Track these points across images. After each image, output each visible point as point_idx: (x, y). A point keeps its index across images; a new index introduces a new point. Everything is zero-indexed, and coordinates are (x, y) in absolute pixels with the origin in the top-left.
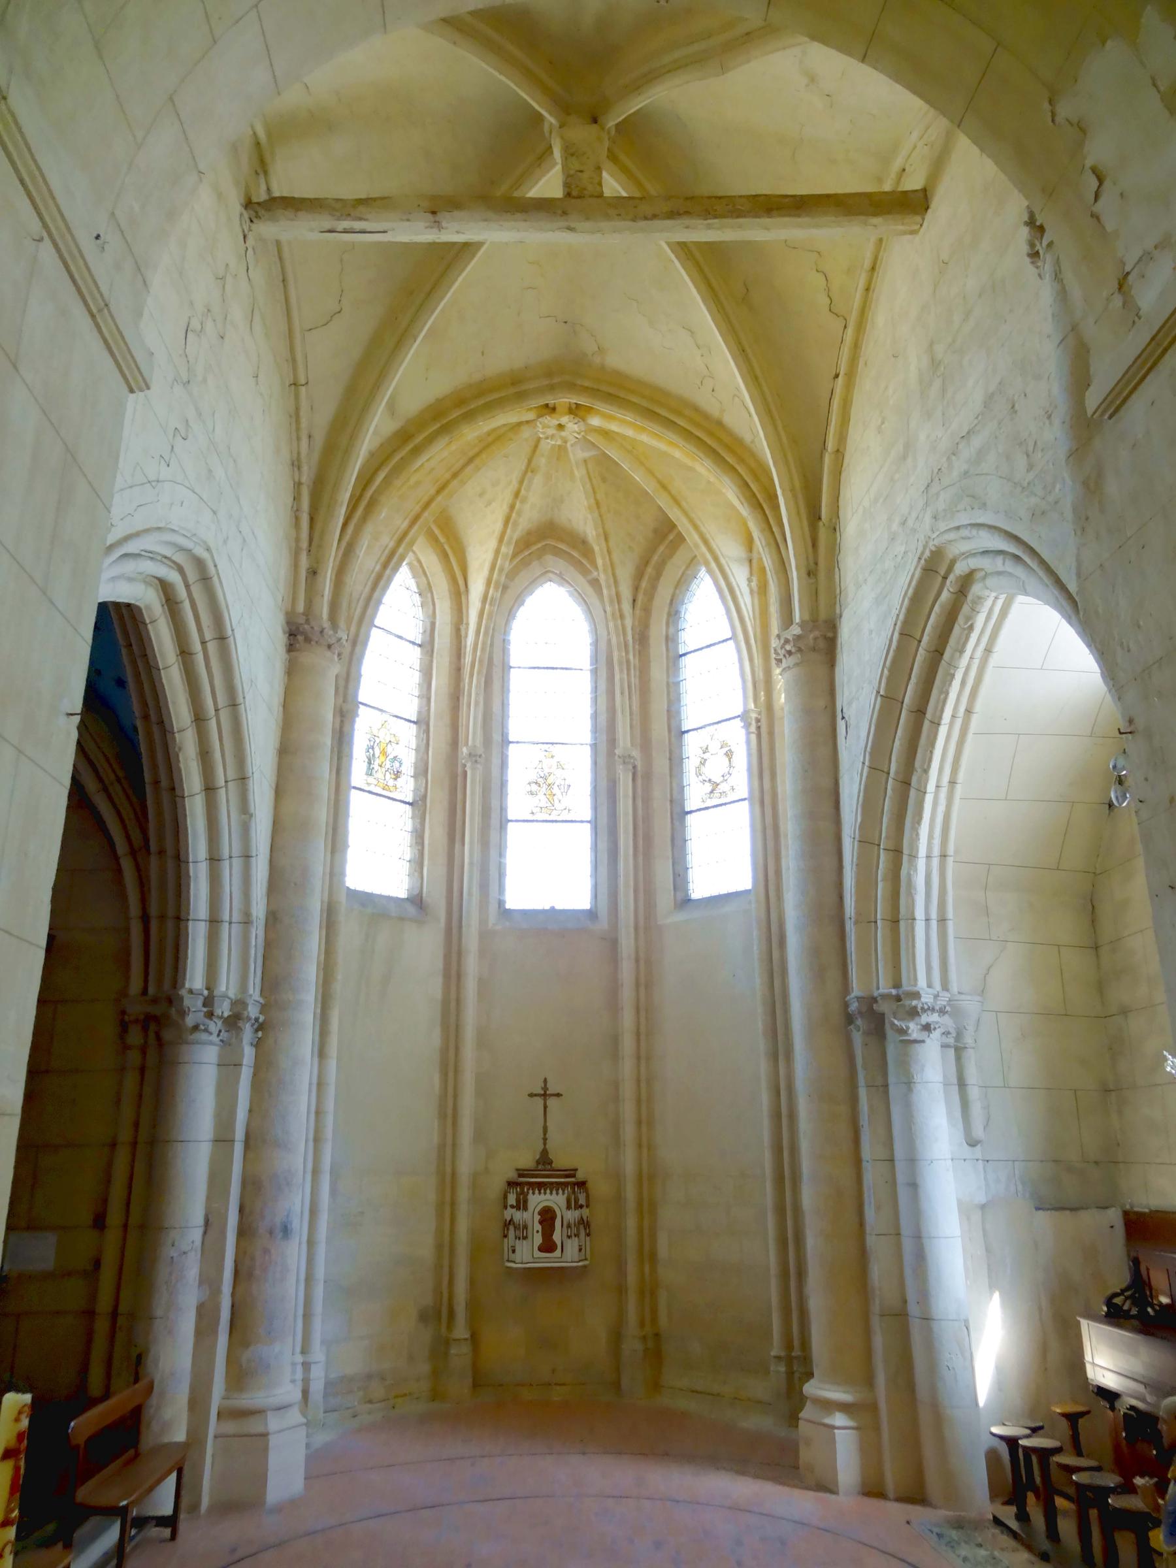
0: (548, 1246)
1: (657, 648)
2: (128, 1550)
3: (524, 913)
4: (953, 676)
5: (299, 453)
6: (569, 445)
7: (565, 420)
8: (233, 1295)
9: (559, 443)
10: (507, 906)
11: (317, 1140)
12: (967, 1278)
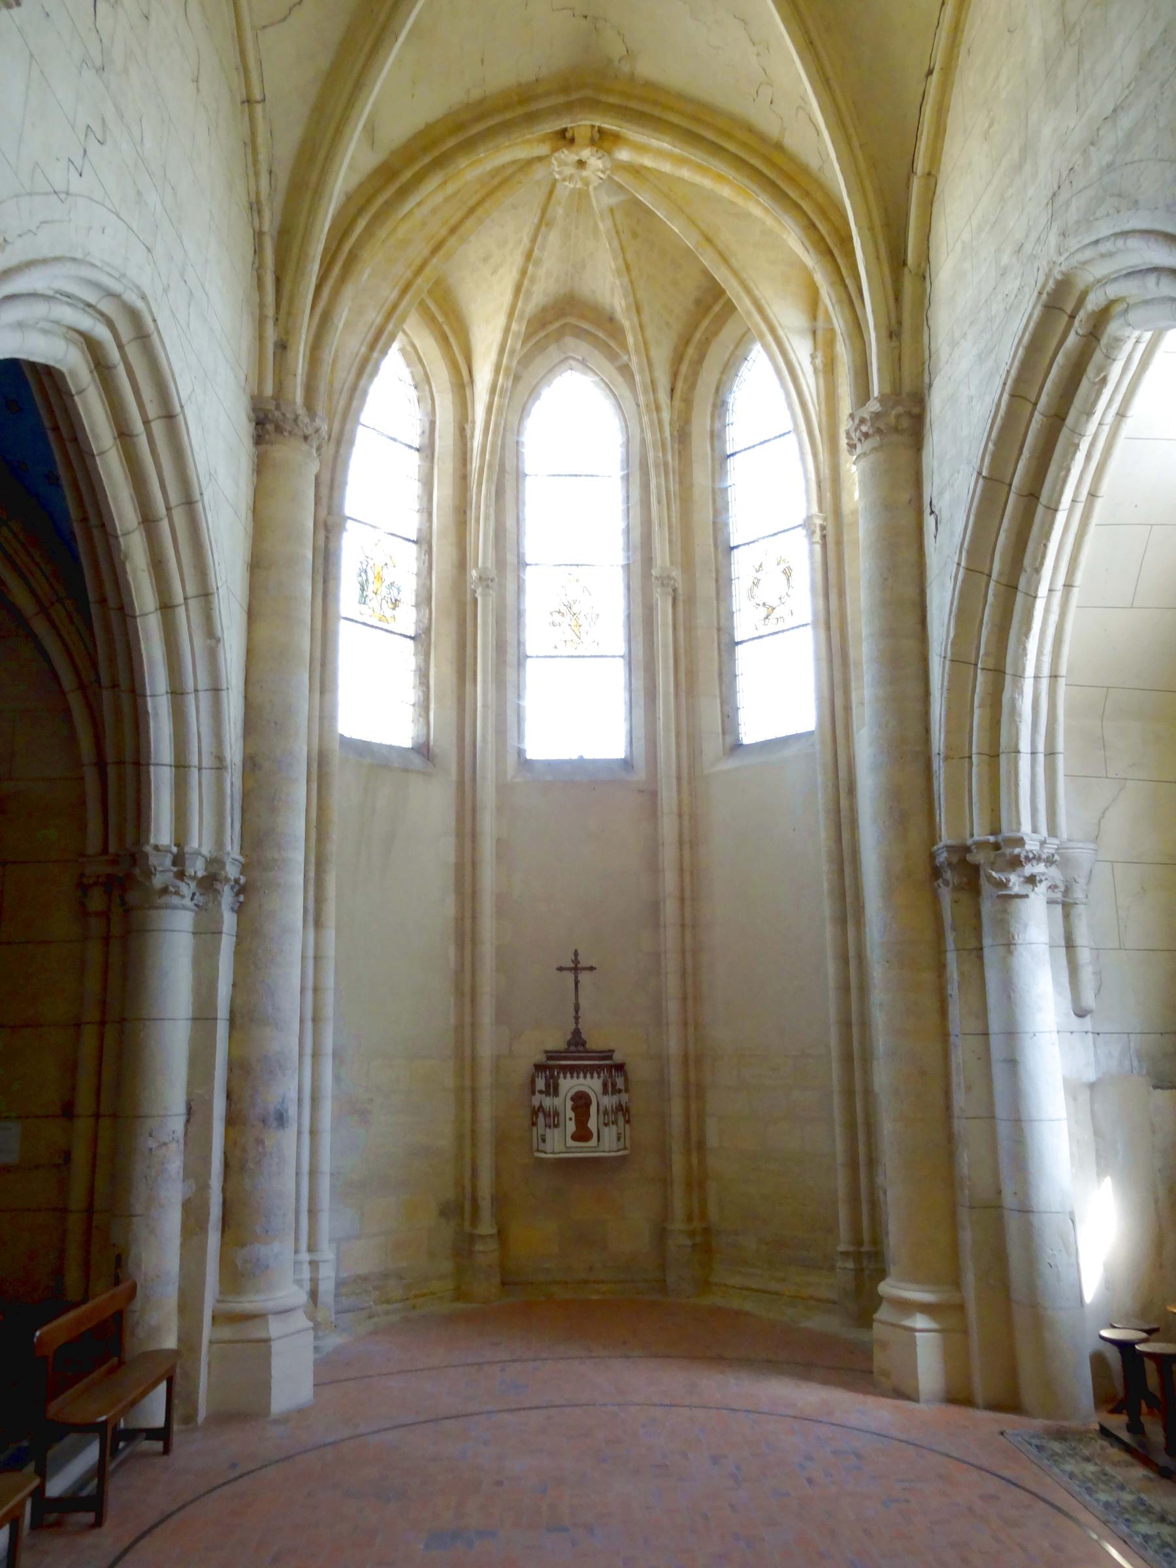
0: (582, 1134)
1: (700, 444)
2: (111, 1467)
3: (550, 765)
4: (1077, 446)
5: (258, 193)
6: (591, 188)
7: (586, 153)
8: (224, 1190)
9: (579, 185)
10: (529, 756)
12: (1072, 1165)
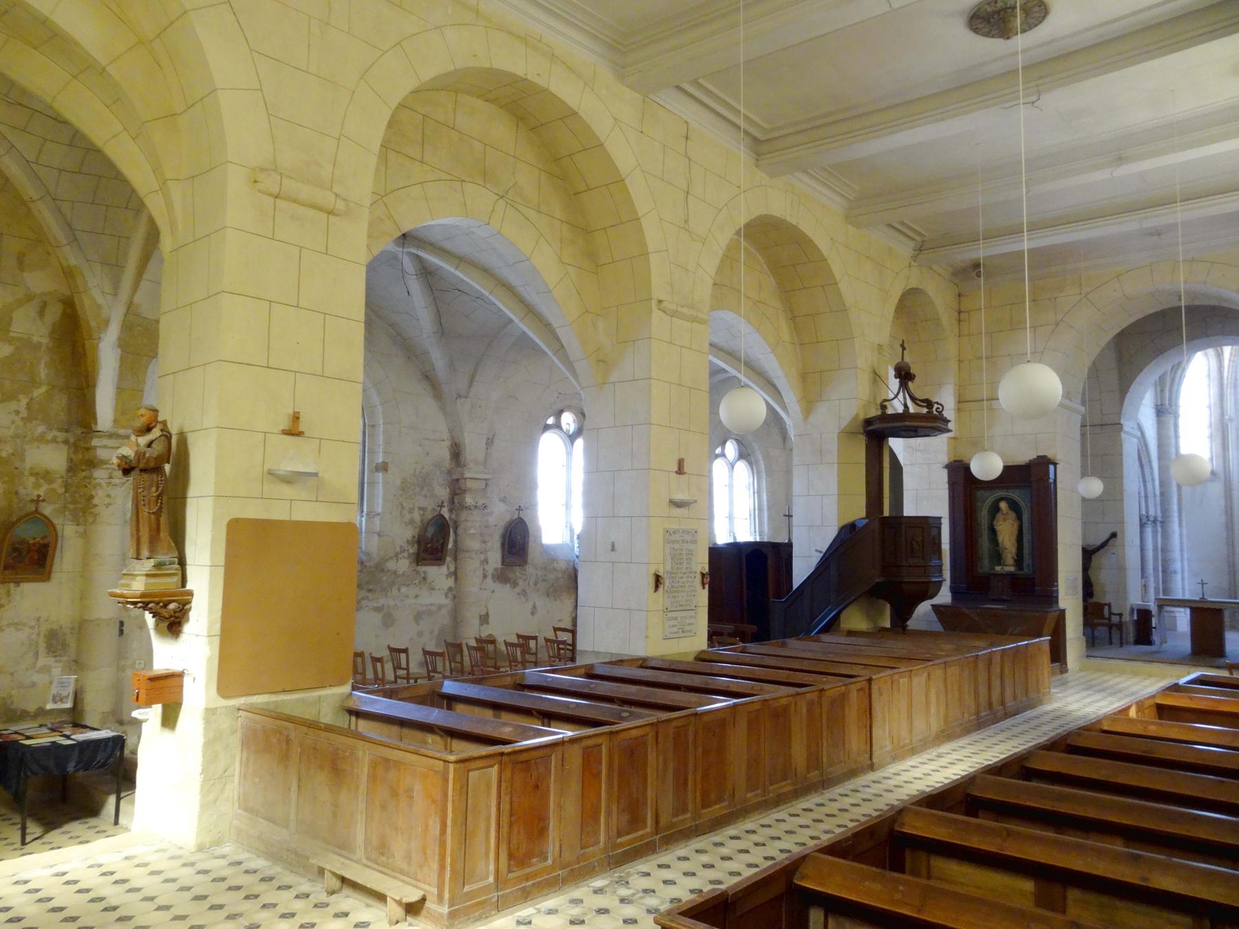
11: (1182, 550)
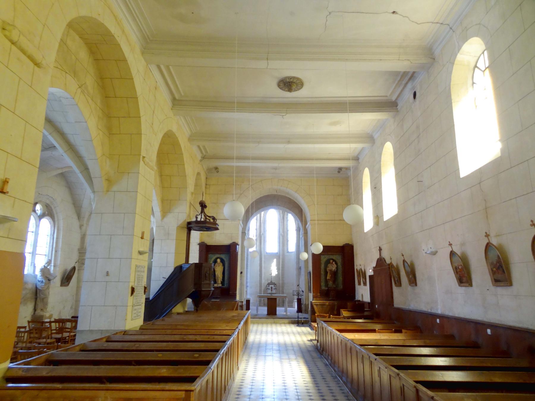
3: (270, 253)
